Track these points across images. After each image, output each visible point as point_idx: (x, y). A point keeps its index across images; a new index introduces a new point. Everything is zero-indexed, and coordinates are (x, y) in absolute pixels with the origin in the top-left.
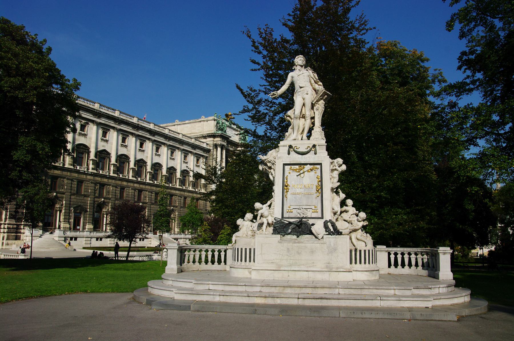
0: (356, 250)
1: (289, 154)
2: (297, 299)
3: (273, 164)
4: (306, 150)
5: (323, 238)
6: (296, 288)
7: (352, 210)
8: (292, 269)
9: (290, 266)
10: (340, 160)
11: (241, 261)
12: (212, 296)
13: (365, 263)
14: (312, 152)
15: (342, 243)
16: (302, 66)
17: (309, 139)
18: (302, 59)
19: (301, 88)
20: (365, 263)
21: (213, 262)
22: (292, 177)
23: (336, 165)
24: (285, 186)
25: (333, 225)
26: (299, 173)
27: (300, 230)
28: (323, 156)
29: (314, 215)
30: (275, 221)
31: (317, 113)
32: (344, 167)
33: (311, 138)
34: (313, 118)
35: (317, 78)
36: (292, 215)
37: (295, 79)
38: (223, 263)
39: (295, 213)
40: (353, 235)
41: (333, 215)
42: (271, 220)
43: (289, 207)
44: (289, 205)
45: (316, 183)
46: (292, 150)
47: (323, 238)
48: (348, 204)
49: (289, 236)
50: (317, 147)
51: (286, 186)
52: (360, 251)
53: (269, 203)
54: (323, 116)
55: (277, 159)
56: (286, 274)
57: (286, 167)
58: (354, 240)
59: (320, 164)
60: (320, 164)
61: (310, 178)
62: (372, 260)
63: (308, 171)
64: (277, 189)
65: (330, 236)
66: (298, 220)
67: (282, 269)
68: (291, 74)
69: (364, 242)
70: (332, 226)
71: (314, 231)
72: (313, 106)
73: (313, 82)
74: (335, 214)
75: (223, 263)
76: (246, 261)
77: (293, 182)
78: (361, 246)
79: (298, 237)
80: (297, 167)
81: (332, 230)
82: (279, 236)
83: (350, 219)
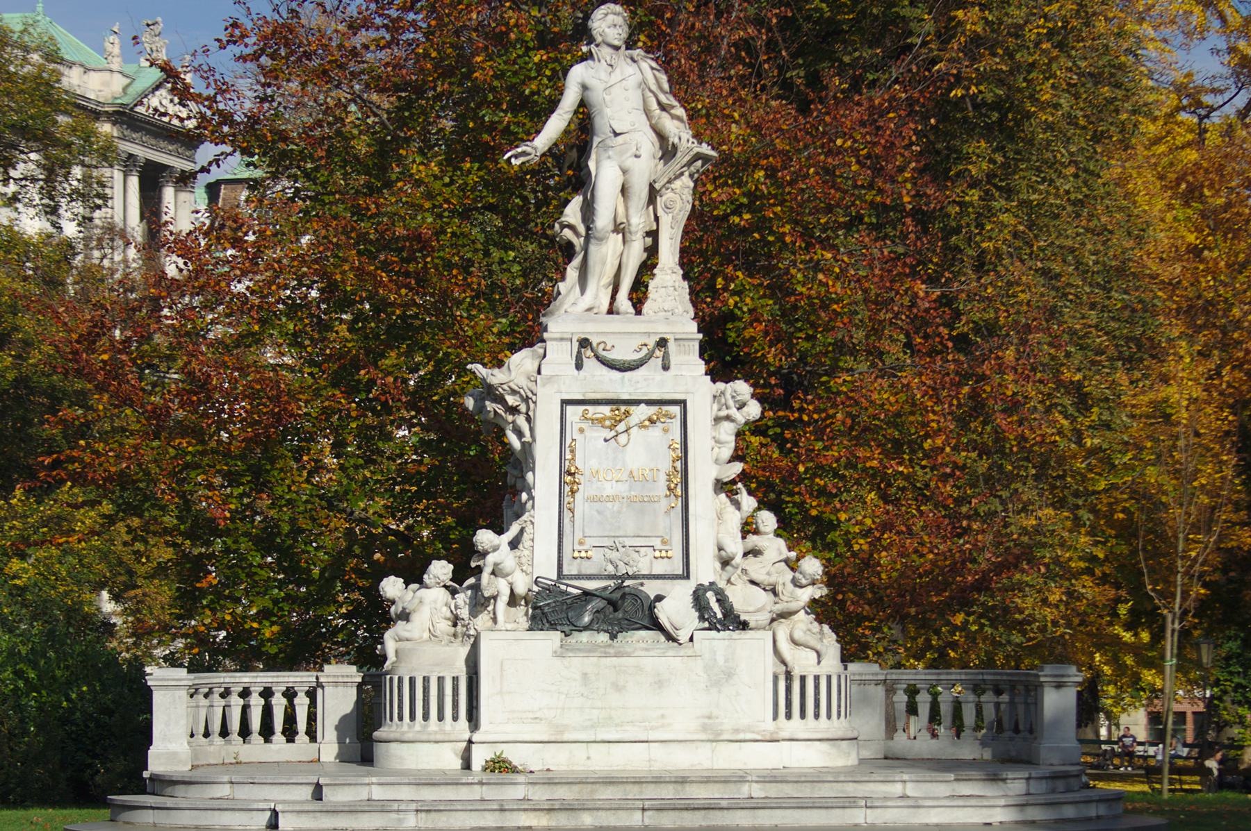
0: (789, 676)
1: (579, 366)
2: (638, 814)
3: (526, 400)
4: (637, 356)
5: (691, 639)
6: (631, 786)
7: (774, 547)
8: (599, 739)
9: (592, 726)
10: (742, 388)
11: (426, 717)
12: (393, 815)
13: (817, 716)
14: (656, 363)
15: (751, 655)
16: (617, 48)
17: (639, 312)
18: (619, 20)
19: (616, 134)
20: (817, 716)
21: (290, 733)
22: (592, 448)
23: (731, 403)
24: (568, 475)
25: (722, 600)
26: (613, 433)
27: (620, 615)
28: (688, 374)
29: (659, 568)
30: (536, 589)
31: (665, 220)
32: (754, 410)
33: (647, 308)
34: (653, 234)
35: (666, 86)
36: (588, 568)
37: (596, 97)
38: (302, 737)
39: (598, 562)
40: (782, 630)
41: (718, 565)
42: (522, 585)
43: (581, 543)
44: (578, 535)
45: (665, 462)
46: (589, 353)
47: (691, 639)
48: (762, 528)
49: (585, 637)
50: (672, 346)
51: (570, 474)
52: (803, 678)
53: (514, 529)
54: (686, 232)
55: (541, 384)
56: (579, 752)
57: (570, 409)
58: (784, 645)
59: (682, 403)
60: (682, 403)
61: (647, 449)
62: (839, 706)
63: (641, 426)
64: (543, 481)
65: (714, 633)
66: (611, 583)
67: (566, 737)
68: (578, 73)
69: (817, 653)
70: (718, 600)
71: (663, 620)
72: (653, 195)
73: (654, 105)
74: (725, 563)
75: (302, 737)
76: (441, 718)
77: (593, 463)
78: (803, 662)
79: (613, 637)
80: (606, 410)
81: (720, 615)
82: (555, 637)
83: (772, 579)
